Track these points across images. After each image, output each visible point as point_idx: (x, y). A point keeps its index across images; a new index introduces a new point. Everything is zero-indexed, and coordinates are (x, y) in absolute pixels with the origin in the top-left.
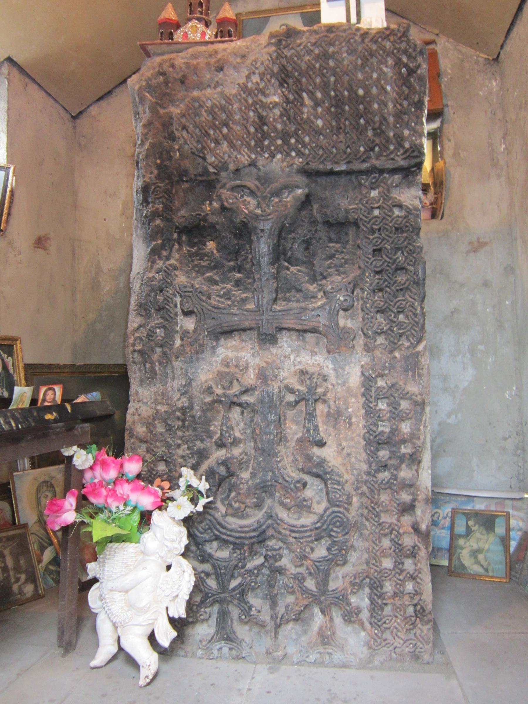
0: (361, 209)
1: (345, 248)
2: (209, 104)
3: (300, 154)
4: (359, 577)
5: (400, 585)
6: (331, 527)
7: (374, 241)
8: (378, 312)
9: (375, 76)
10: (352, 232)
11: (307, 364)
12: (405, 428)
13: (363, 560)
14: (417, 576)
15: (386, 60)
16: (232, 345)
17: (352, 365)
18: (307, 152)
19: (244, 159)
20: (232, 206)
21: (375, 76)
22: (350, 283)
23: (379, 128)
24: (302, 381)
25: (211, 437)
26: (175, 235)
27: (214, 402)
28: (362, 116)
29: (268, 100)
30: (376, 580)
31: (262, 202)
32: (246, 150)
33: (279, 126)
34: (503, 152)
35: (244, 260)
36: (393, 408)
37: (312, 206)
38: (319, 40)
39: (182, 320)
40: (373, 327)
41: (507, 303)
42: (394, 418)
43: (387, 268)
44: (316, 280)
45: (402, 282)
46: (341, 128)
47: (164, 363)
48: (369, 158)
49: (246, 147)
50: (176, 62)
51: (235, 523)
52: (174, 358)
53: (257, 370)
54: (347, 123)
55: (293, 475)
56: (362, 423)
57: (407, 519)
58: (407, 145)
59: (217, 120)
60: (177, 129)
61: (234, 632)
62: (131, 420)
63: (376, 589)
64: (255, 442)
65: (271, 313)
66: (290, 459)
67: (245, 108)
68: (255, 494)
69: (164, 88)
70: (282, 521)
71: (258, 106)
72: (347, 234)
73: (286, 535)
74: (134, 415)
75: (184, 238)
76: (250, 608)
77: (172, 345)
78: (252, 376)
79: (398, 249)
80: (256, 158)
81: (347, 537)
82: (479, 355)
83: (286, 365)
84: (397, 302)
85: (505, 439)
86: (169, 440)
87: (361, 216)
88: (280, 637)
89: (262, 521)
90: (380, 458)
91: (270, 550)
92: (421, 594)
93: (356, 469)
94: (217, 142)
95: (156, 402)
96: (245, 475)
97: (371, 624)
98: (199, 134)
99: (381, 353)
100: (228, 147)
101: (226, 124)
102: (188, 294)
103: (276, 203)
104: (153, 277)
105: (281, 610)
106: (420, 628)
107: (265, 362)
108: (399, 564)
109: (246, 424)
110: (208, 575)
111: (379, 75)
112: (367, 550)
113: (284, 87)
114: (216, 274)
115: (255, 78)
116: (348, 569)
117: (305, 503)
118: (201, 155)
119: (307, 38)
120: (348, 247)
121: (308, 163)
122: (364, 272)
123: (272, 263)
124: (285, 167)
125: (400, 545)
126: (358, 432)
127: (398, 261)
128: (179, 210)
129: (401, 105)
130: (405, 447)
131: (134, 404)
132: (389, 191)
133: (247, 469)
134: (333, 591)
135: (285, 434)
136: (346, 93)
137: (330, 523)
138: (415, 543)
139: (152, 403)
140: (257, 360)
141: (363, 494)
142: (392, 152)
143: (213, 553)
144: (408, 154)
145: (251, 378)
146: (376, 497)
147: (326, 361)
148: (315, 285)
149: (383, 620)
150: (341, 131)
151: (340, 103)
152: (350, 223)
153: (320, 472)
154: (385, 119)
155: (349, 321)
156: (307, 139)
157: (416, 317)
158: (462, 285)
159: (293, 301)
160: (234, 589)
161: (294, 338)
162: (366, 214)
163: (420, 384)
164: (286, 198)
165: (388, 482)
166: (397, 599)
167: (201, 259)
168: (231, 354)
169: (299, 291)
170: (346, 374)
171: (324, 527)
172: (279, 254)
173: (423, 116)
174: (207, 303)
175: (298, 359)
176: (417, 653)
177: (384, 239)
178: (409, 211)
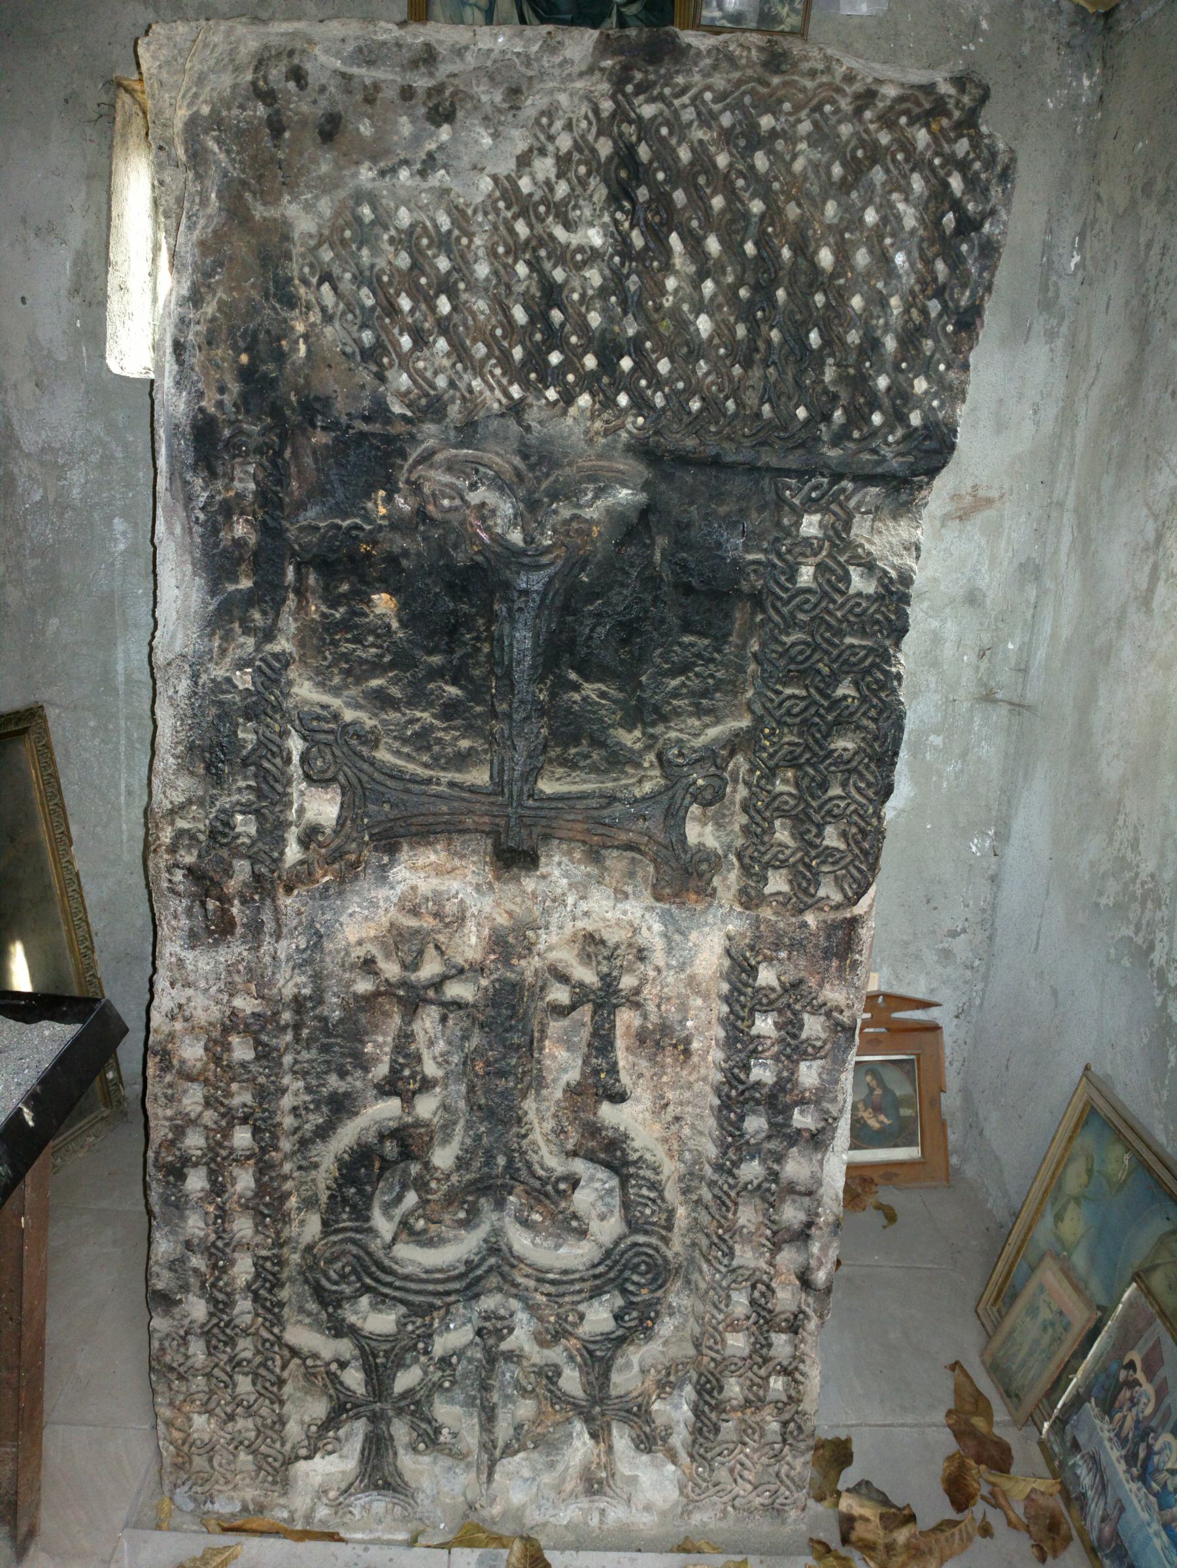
0: (774, 566)
1: (719, 651)
2: (404, 217)
3: (640, 404)
7: (793, 652)
9: (871, 216)
10: (740, 615)
11: (604, 920)
12: (809, 1074)
15: (906, 177)
18: (659, 400)
19: (494, 401)
20: (449, 516)
23: (859, 365)
25: (366, 1070)
27: (377, 994)
29: (575, 239)
32: (498, 371)
33: (595, 319)
35: (467, 656)
37: (651, 538)
39: (302, 793)
42: (788, 1057)
45: (846, 755)
46: (757, 350)
49: (499, 363)
51: (412, 1262)
53: (486, 932)
56: (717, 1055)
57: (788, 1258)
58: (915, 419)
59: (424, 274)
60: (305, 282)
61: (400, 1475)
62: (166, 1029)
63: (710, 1393)
64: (471, 1089)
66: (549, 1125)
67: (507, 253)
69: (268, 143)
70: (521, 1260)
71: (543, 253)
72: (728, 616)
75: (312, 580)
76: (438, 1431)
78: (473, 940)
80: (522, 399)
81: (659, 1294)
86: (262, 1080)
87: (772, 584)
88: (497, 1476)
92: (800, 1401)
94: (421, 340)
96: (443, 1157)
97: (691, 1456)
98: (370, 302)
99: (776, 913)
100: (448, 355)
101: (446, 286)
102: (322, 737)
105: (503, 1430)
107: (510, 914)
108: (760, 1351)
109: (449, 1043)
111: (884, 220)
112: (699, 1319)
113: (621, 208)
114: (395, 681)
115: (545, 167)
117: (574, 1224)
119: (706, 75)
120: (727, 649)
123: (542, 680)
126: (703, 1071)
128: (301, 506)
129: (924, 312)
130: (802, 1112)
131: (174, 992)
132: (848, 526)
133: (446, 1141)
136: (786, 253)
139: (220, 991)
140: (487, 904)
142: (875, 433)
143: (359, 1324)
145: (470, 944)
148: (637, 733)
152: (739, 592)
153: (612, 1153)
155: (710, 828)
156: (664, 366)
159: (582, 769)
161: (577, 855)
165: (759, 1186)
167: (357, 640)
168: (426, 885)
169: (596, 743)
170: (691, 954)
171: (612, 1275)
172: (560, 653)
174: (372, 764)
175: (584, 906)
177: (816, 647)
178: (884, 579)
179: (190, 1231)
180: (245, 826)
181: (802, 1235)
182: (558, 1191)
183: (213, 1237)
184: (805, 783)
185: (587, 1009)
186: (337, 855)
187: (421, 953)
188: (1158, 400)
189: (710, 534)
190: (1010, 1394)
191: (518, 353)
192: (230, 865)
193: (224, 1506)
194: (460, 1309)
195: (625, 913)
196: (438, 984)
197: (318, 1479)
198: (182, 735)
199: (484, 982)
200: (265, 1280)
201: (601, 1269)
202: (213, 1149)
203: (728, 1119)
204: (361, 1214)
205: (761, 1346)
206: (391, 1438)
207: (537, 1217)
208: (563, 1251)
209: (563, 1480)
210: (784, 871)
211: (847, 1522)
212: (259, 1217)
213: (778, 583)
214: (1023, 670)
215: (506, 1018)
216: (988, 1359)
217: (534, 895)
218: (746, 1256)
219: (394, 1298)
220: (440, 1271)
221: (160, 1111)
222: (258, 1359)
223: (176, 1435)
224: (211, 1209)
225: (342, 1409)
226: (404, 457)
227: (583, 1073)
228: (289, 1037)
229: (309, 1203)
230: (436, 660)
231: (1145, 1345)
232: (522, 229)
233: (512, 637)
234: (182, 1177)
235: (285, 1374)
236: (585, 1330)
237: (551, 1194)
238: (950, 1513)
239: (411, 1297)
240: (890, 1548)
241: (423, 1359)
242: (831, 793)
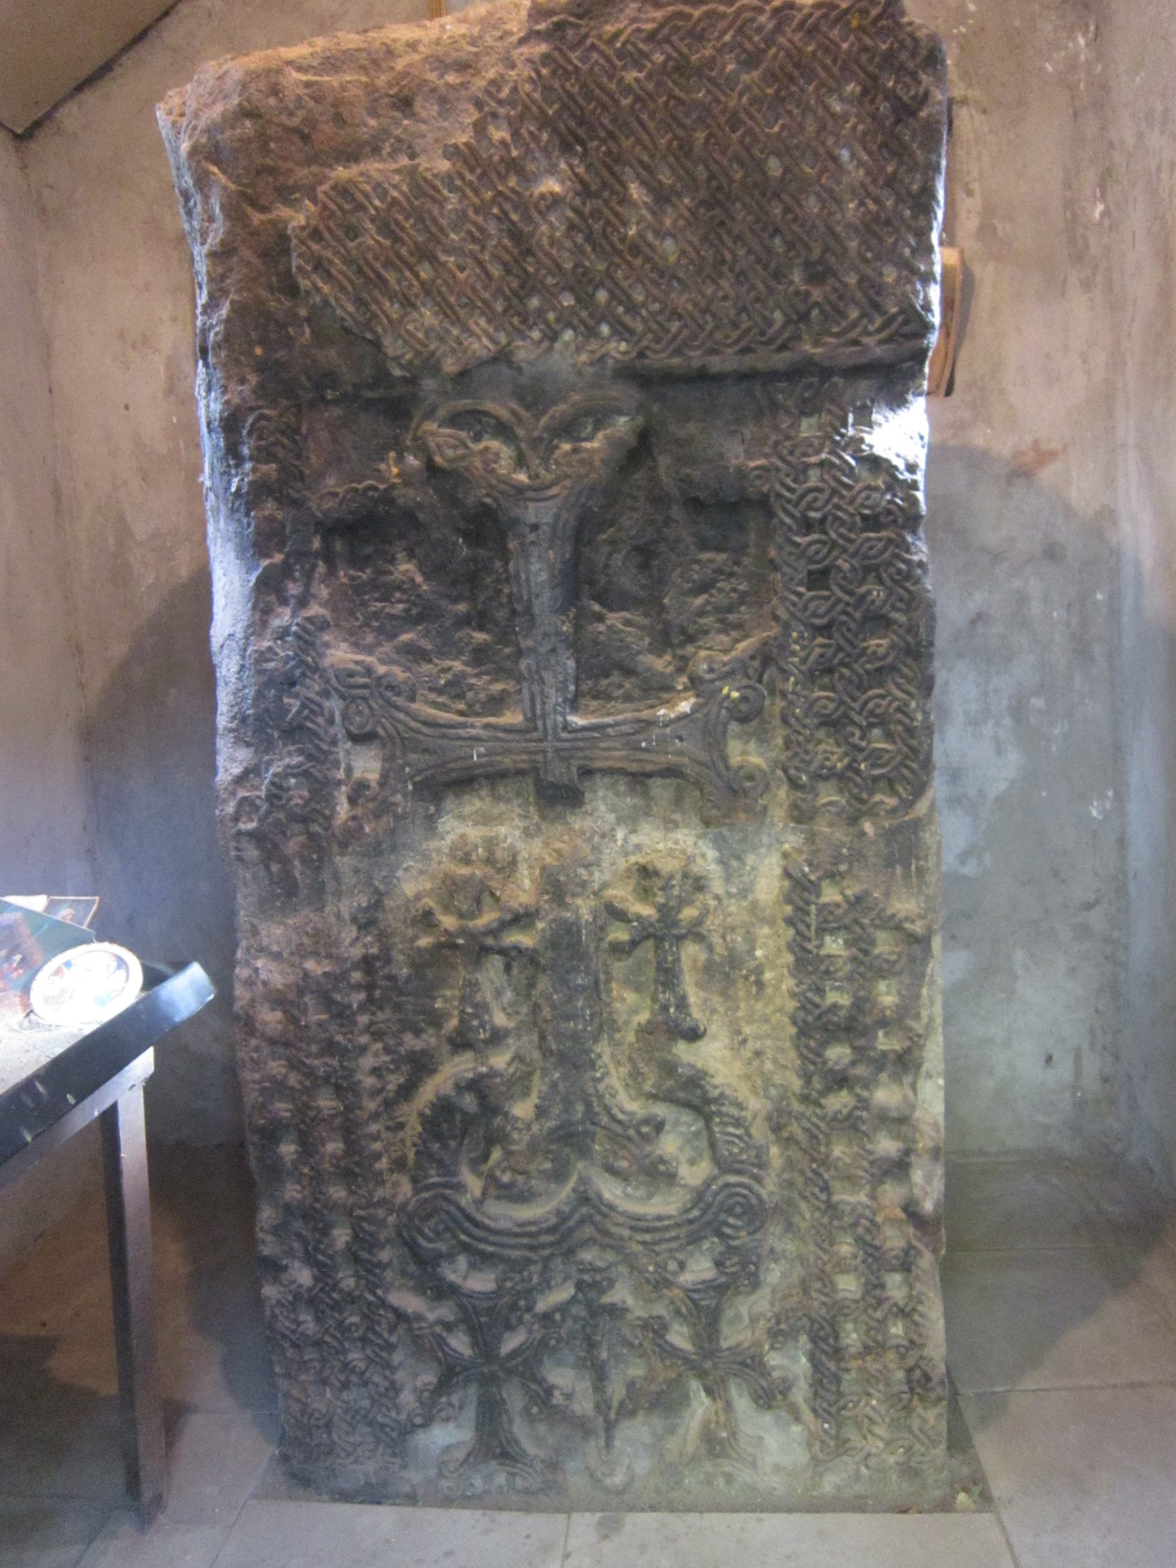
0: (778, 470)
1: (737, 563)
3: (621, 330)
4: (787, 1318)
5: (878, 1331)
6: (722, 1217)
8: (822, 724)
13: (794, 1279)
14: (914, 1309)
16: (474, 809)
17: (763, 850)
22: (753, 657)
24: (645, 890)
26: (316, 544)
27: (438, 946)
28: (777, 231)
30: (823, 1323)
31: (529, 454)
32: (483, 322)
34: (1100, 224)
35: (492, 598)
36: (860, 950)
37: (654, 459)
38: (662, 26)
39: (348, 753)
40: (811, 762)
41: (1099, 597)
42: (860, 974)
43: (844, 618)
44: (671, 645)
45: (881, 651)
46: (724, 262)
47: (312, 860)
48: (797, 338)
50: (283, 81)
51: (505, 1217)
52: (335, 848)
53: (537, 871)
56: (789, 984)
57: (892, 1193)
62: (248, 995)
63: (825, 1340)
64: (542, 1037)
65: (565, 735)
66: (624, 1070)
68: (549, 1152)
70: (612, 1207)
72: (742, 529)
73: (621, 1238)
76: (549, 1391)
77: (329, 819)
78: (527, 883)
79: (867, 570)
81: (758, 1236)
82: (1033, 721)
84: (866, 702)
85: (1088, 907)
86: (339, 1038)
87: (778, 487)
88: (617, 1443)
89: (567, 1209)
90: (830, 1063)
91: (587, 1271)
92: (922, 1346)
93: (774, 1085)
94: (408, 304)
95: (301, 952)
96: (522, 1110)
97: (814, 1410)
99: (831, 825)
103: (566, 454)
104: (270, 649)
105: (616, 1391)
106: (919, 1416)
107: (559, 852)
110: (449, 1327)
113: (575, 154)
114: (426, 634)
117: (662, 1168)
118: (369, 336)
120: (746, 561)
121: (641, 355)
122: (787, 627)
123: (563, 610)
124: (584, 363)
125: (877, 1248)
127: (869, 598)
128: (320, 475)
130: (886, 1034)
133: (526, 1093)
134: (729, 1349)
135: (611, 1013)
137: (721, 1209)
138: (909, 1242)
140: (536, 847)
141: (790, 1141)
142: (854, 325)
144: (893, 327)
145: (523, 890)
146: (823, 1149)
147: (700, 843)
148: (668, 657)
149: (841, 1403)
150: (725, 268)
151: (720, 196)
152: (749, 501)
153: (694, 1095)
155: (752, 745)
157: (912, 737)
158: (997, 557)
159: (616, 699)
160: (514, 1354)
161: (622, 788)
162: (789, 481)
163: (920, 892)
164: (589, 439)
166: (868, 1358)
167: (385, 598)
168: (474, 833)
169: (629, 672)
170: (750, 878)
171: (707, 1218)
172: (580, 583)
173: (931, 228)
174: (407, 713)
175: (634, 839)
176: (912, 1464)
177: (834, 545)
182: (639, 1133)
183: (309, 1201)
187: (478, 901)
198: (236, 709)
202: (302, 1110)
203: (807, 1047)
204: (448, 1170)
205: (874, 1286)
208: (656, 1199)
213: (783, 485)
219: (492, 1255)
225: (451, 1375)
227: (653, 1012)
228: (362, 996)
229: (399, 1164)
230: (462, 607)
233: (528, 572)
239: (507, 1252)
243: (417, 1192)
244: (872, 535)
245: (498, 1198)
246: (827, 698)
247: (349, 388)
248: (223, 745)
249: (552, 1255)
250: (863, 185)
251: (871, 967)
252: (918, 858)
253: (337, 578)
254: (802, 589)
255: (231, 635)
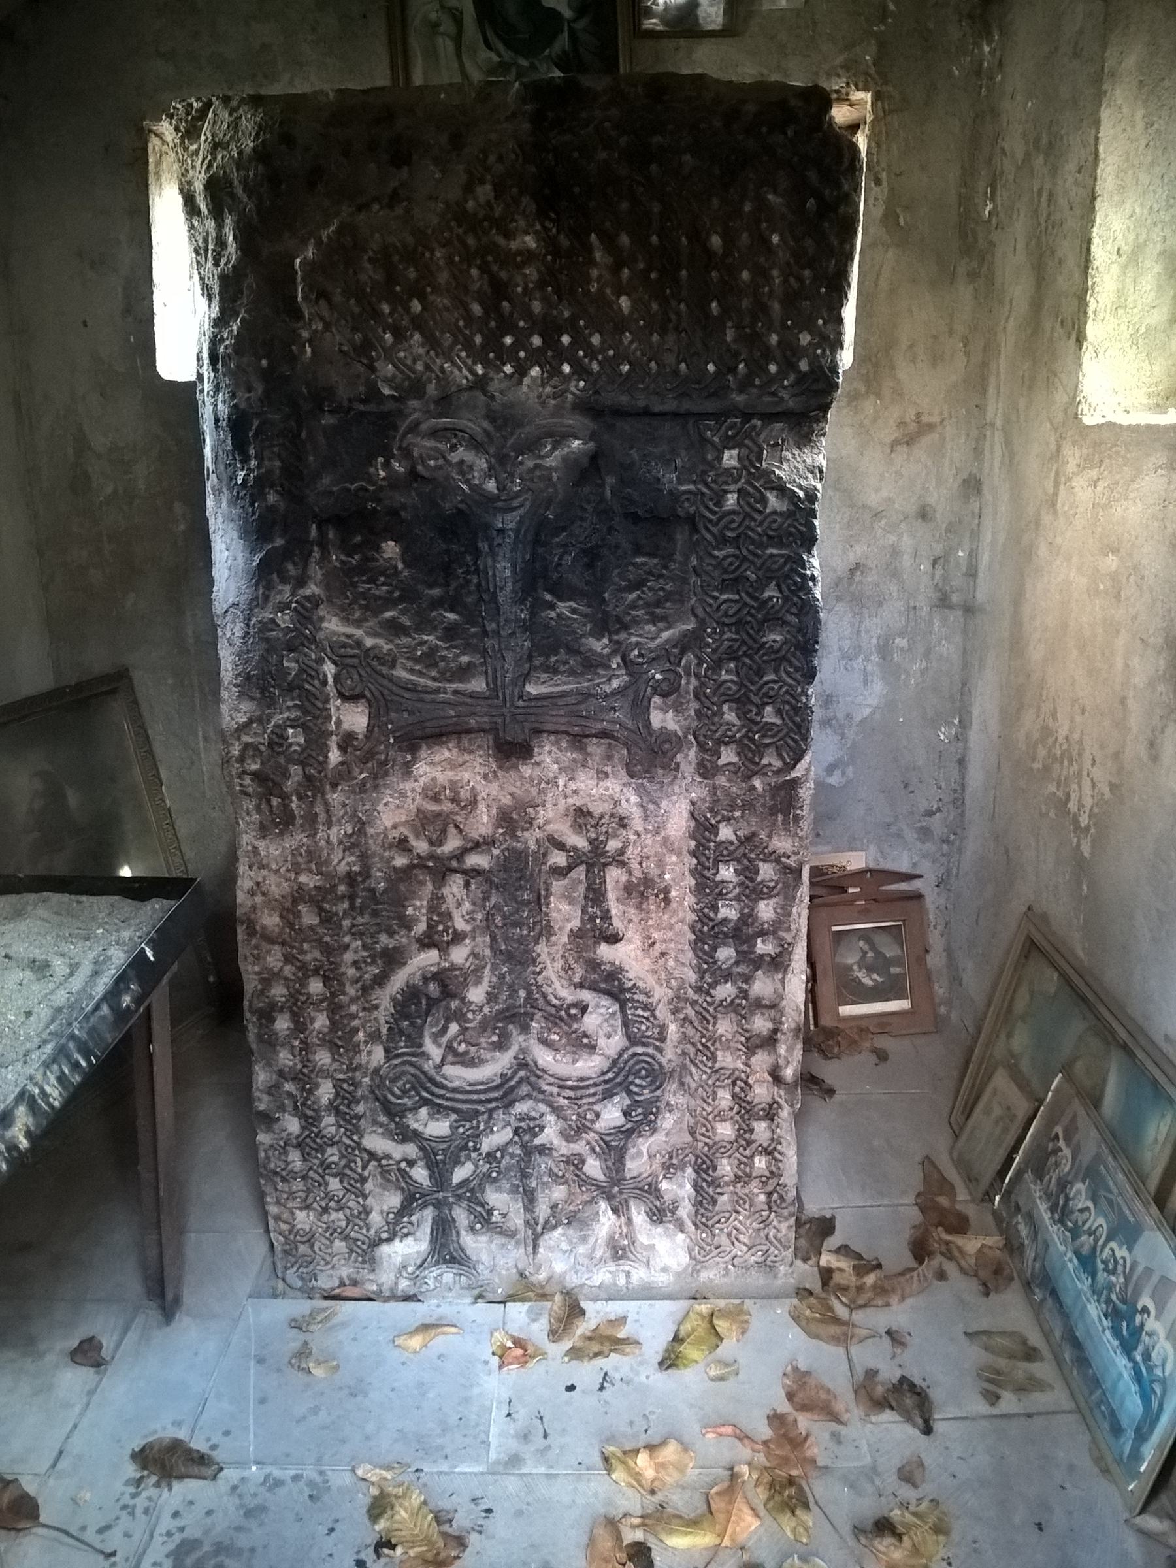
0: (703, 494)
1: (666, 567)
3: (580, 371)
7: (726, 563)
9: (748, 208)
10: (681, 537)
11: (590, 796)
12: (766, 910)
18: (595, 366)
19: (462, 377)
21: (748, 208)
25: (409, 929)
27: (411, 867)
29: (514, 245)
32: (463, 354)
33: (537, 307)
35: (461, 586)
39: (338, 709)
45: (776, 646)
46: (670, 320)
49: (464, 348)
54: (682, 306)
55: (563, 993)
56: (690, 900)
57: (761, 1060)
58: (804, 366)
61: (463, 1250)
62: (249, 903)
64: (493, 939)
65: (521, 703)
66: (559, 964)
70: (544, 1071)
72: (671, 539)
74: (252, 893)
76: (490, 1212)
78: (485, 819)
79: (772, 578)
81: (658, 1093)
83: (549, 799)
85: (930, 814)
86: (327, 939)
87: (702, 509)
88: (541, 1250)
94: (400, 335)
96: (476, 994)
97: (695, 1224)
98: (357, 310)
99: (729, 781)
102: (348, 661)
103: (531, 471)
104: (273, 621)
105: (542, 1210)
109: (474, 904)
114: (404, 612)
115: (485, 191)
116: (660, 1137)
117: (585, 1041)
120: (672, 566)
123: (522, 601)
126: (681, 915)
129: (800, 279)
131: (252, 873)
133: (478, 982)
140: (493, 789)
142: (772, 379)
143: (421, 1129)
145: (483, 823)
148: (605, 641)
153: (611, 984)
154: (765, 309)
155: (671, 714)
156: (596, 340)
157: (796, 714)
158: (877, 515)
159: (562, 673)
161: (564, 745)
162: (711, 504)
164: (549, 454)
165: (732, 1001)
167: (372, 580)
168: (443, 777)
169: (573, 651)
170: (662, 820)
172: (536, 580)
174: (391, 680)
175: (573, 786)
179: (281, 1062)
180: (296, 737)
181: (770, 1041)
182: (569, 1015)
183: (299, 1066)
184: (743, 672)
185: (582, 868)
186: (369, 756)
187: (444, 831)
188: (1053, 328)
189: (649, 471)
190: (971, 1179)
191: (478, 339)
192: (287, 769)
193: (326, 1281)
194: (500, 1115)
195: (607, 789)
196: (460, 855)
197: (399, 1259)
198: (240, 668)
199: (496, 852)
200: (344, 1098)
201: (610, 1075)
202: (294, 996)
204: (415, 1042)
206: (454, 1220)
207: (555, 1037)
208: (579, 1064)
209: (594, 1249)
210: (734, 746)
211: (826, 1275)
212: (334, 1048)
213: (707, 508)
214: (972, 573)
215: (516, 881)
216: (955, 1155)
217: (531, 779)
218: (726, 1059)
219: (447, 1108)
220: (482, 1083)
221: (250, 968)
222: (343, 1162)
223: (284, 1227)
224: (296, 1043)
225: (412, 1200)
226: (395, 428)
227: (582, 920)
228: (346, 905)
229: (374, 1037)
231: (1065, 1120)
232: (471, 241)
233: (495, 568)
234: (273, 1021)
235: (366, 1173)
236: (600, 1125)
237: (565, 1020)
238: (913, 1263)
239: (459, 1106)
240: (860, 1289)
241: (474, 1155)
242: (765, 679)
243: (388, 1059)
244: (775, 552)
245: (452, 1063)
246: (732, 681)
247: (346, 403)
248: (228, 695)
249: (497, 1108)
250: (788, 264)
251: (753, 891)
252: (795, 808)
253: (330, 562)
254: (716, 594)
255: (235, 605)
